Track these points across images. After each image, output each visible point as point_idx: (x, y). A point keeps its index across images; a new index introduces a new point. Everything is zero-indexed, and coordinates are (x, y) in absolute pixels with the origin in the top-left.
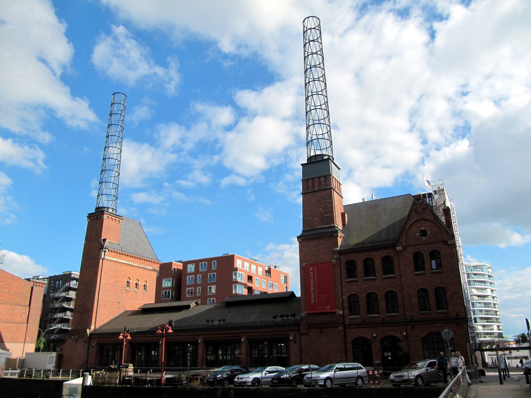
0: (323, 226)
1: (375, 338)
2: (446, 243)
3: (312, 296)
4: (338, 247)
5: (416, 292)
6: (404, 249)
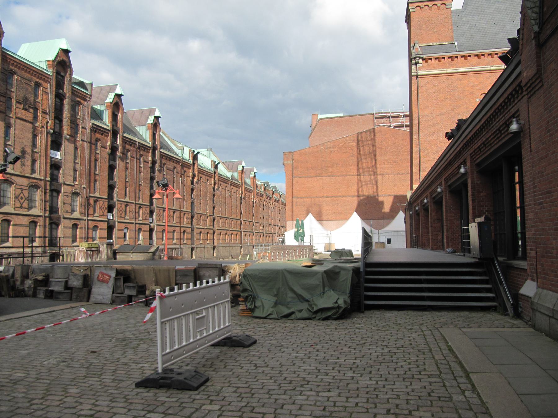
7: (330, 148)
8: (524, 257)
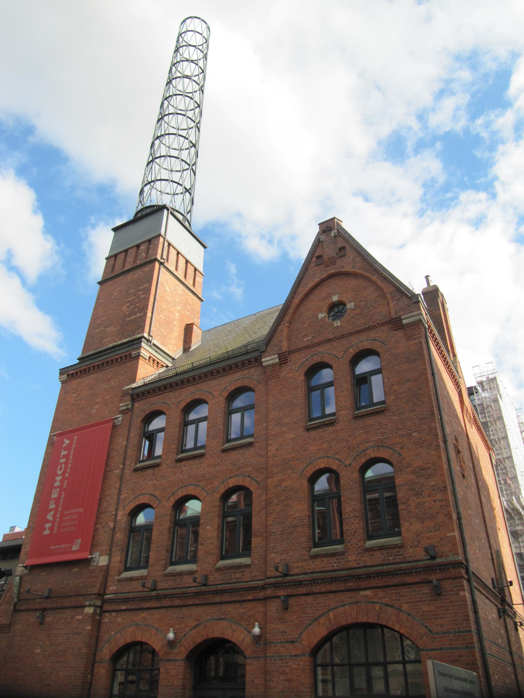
0: (119, 342)
1: (171, 644)
2: (396, 323)
3: (50, 517)
4: (134, 381)
5: (305, 483)
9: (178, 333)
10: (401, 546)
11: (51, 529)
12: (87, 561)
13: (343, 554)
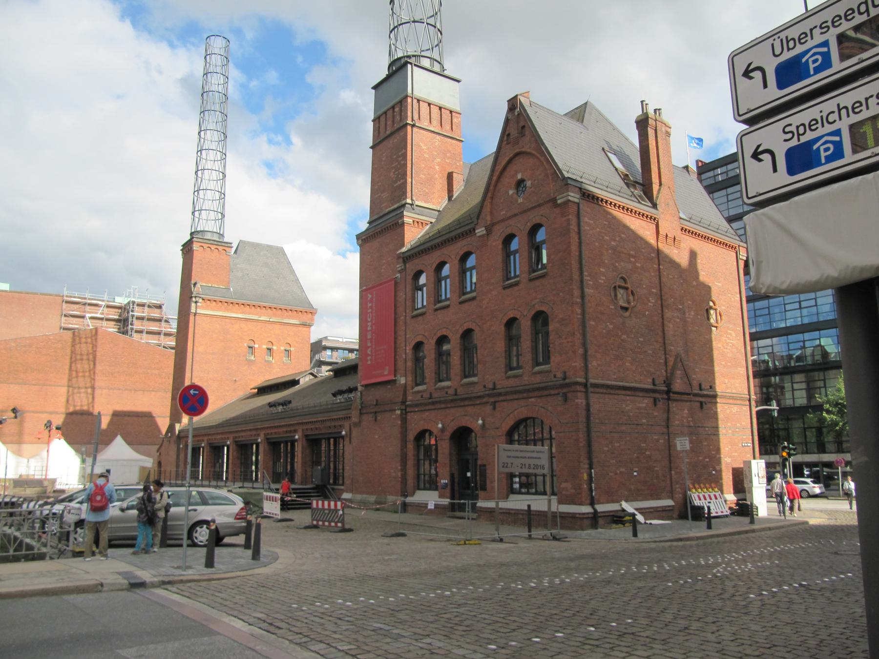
0: (392, 208)
3: (369, 352)
4: (403, 245)
6: (489, 230)
7: (25, 346)
8: (343, 484)
9: (441, 184)
10: (549, 372)
11: (371, 360)
12: (394, 381)
13: (521, 376)
